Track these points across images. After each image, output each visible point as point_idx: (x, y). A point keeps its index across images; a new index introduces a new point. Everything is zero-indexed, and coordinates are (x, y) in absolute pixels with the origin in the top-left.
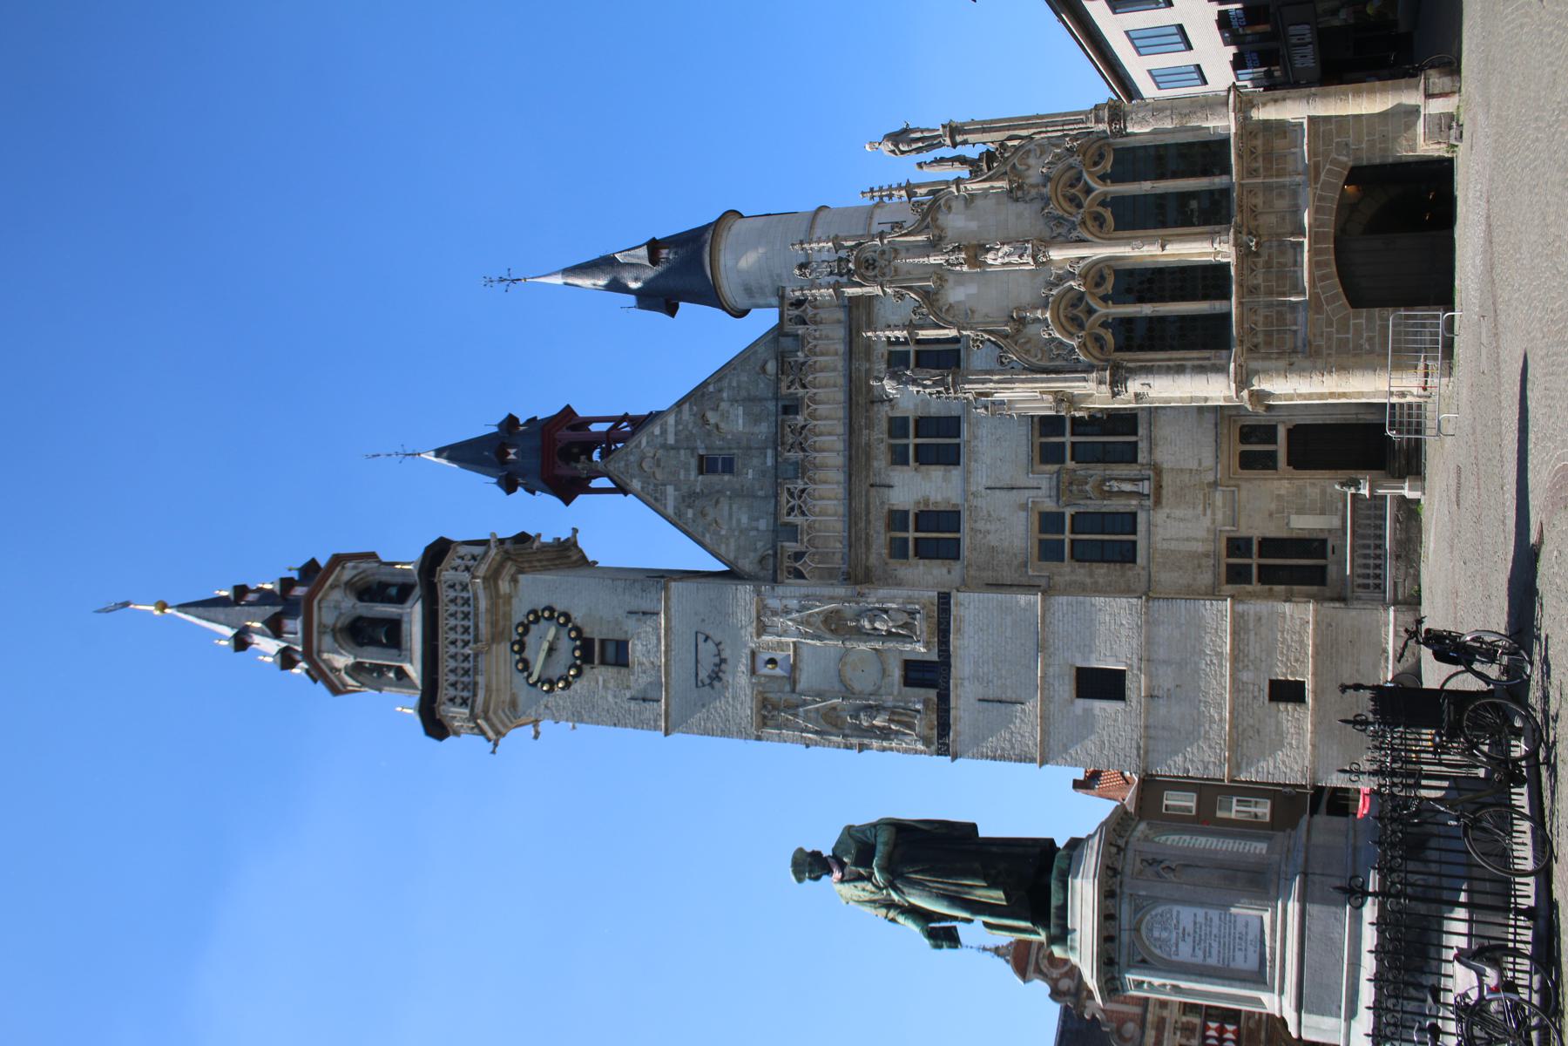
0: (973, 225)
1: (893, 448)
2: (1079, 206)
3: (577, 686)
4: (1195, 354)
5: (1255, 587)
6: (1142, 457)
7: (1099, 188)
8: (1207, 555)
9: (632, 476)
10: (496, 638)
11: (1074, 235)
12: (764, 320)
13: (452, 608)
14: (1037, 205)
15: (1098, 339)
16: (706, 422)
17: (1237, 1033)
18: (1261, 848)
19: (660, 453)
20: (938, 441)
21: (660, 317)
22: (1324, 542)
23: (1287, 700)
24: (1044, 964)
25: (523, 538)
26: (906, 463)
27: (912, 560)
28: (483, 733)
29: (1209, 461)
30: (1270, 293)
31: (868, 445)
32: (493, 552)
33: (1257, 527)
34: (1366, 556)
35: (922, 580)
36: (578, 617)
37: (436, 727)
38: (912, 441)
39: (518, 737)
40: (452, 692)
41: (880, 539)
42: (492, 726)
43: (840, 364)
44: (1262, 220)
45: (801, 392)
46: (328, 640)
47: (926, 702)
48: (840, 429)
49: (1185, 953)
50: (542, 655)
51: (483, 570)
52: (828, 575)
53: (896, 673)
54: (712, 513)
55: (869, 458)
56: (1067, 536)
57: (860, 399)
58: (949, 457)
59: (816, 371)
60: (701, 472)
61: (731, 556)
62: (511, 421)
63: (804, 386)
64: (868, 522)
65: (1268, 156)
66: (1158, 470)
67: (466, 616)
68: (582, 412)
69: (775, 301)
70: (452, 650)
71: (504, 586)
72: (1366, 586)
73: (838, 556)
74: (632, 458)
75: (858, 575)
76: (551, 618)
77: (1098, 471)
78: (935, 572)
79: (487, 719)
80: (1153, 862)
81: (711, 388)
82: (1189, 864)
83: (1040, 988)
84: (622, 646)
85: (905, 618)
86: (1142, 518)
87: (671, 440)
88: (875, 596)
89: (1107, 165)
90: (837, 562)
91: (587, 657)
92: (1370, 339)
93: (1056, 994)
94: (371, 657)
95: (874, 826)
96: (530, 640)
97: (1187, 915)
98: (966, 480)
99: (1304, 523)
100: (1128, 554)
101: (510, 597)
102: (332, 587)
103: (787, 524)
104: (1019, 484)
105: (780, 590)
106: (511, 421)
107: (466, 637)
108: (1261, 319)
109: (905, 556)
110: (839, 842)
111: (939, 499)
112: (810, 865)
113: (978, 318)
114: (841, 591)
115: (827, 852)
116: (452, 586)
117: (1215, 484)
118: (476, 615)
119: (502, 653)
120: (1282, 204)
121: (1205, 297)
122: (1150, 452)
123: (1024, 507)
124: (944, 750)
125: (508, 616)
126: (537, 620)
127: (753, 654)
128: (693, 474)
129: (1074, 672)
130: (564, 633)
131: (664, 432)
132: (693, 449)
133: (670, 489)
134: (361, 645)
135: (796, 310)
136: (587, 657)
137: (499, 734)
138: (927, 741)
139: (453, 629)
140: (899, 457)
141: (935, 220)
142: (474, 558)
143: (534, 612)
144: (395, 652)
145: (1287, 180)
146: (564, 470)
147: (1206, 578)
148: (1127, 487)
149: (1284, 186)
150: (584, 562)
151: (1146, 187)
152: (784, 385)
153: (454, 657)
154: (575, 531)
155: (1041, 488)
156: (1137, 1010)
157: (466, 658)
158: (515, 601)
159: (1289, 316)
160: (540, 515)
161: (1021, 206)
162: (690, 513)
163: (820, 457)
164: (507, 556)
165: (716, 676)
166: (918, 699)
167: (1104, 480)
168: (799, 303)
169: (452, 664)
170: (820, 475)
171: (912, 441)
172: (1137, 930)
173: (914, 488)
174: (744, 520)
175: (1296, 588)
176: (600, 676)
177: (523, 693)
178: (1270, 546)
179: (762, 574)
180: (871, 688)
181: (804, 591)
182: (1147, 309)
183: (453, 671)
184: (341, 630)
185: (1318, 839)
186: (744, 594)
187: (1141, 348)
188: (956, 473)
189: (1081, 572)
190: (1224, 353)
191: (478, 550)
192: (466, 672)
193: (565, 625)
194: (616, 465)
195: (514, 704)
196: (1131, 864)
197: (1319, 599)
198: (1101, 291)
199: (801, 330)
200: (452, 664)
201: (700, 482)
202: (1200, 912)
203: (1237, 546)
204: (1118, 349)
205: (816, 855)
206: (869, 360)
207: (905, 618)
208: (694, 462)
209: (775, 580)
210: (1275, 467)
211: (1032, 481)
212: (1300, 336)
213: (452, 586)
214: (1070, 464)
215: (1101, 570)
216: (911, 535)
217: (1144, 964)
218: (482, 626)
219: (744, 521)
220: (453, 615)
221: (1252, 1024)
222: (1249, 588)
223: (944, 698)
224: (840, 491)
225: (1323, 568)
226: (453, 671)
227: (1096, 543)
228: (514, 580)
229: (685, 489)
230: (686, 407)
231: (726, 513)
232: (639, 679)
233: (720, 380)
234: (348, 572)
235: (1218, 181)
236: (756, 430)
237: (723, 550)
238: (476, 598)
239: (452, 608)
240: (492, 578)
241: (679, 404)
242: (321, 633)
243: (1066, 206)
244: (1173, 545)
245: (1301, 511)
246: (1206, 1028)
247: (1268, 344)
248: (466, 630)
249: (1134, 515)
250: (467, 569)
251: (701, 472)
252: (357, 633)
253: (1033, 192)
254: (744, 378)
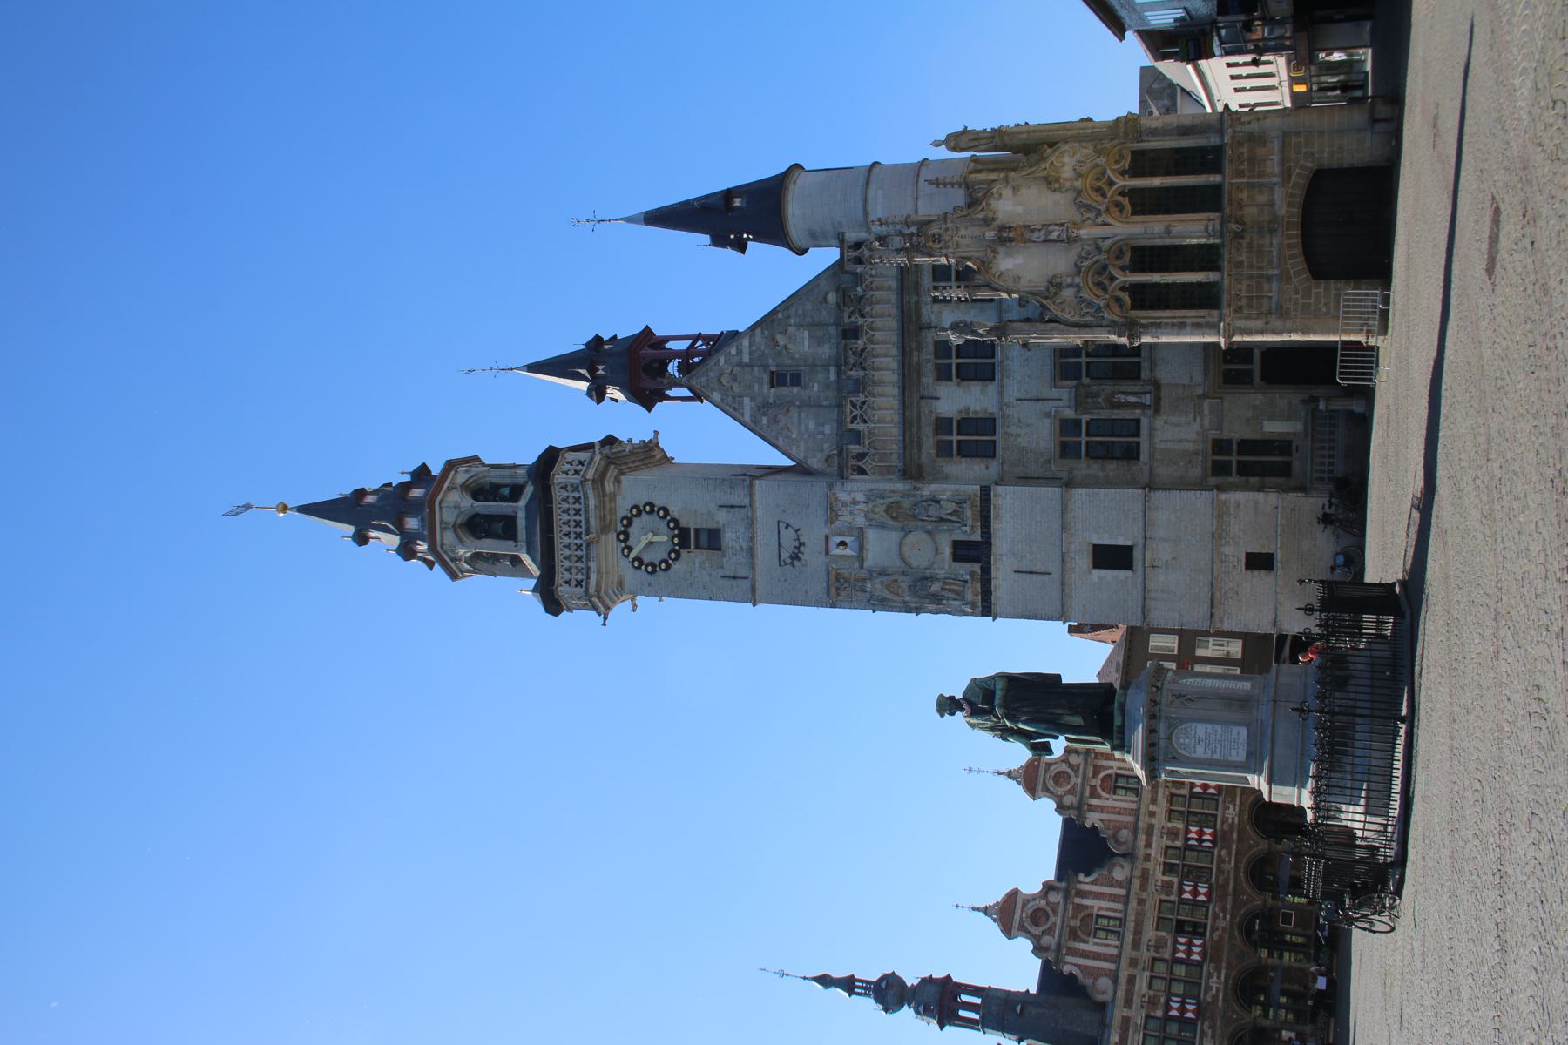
0: (1020, 209)
1: (938, 367)
2: (1104, 195)
3: (676, 566)
4: (1193, 313)
5: (1234, 479)
6: (1145, 374)
7: (1121, 182)
8: (1196, 453)
9: (713, 390)
10: (605, 529)
11: (1100, 220)
12: (824, 257)
13: (565, 506)
14: (1070, 196)
15: (1118, 300)
16: (776, 344)
17: (1214, 835)
18: (1247, 685)
19: (736, 370)
20: (977, 363)
21: (729, 253)
22: (1290, 442)
23: (1259, 568)
24: (1050, 784)
25: (610, 441)
26: (950, 379)
27: (956, 459)
28: (595, 608)
29: (1198, 378)
30: (1251, 267)
31: (918, 364)
32: (597, 458)
33: (1237, 430)
34: (1323, 456)
35: (964, 476)
36: (675, 511)
37: (553, 606)
38: (954, 361)
39: (621, 610)
40: (567, 576)
41: (929, 442)
42: (603, 603)
43: (893, 297)
44: (1247, 210)
45: (861, 321)
46: (449, 537)
47: (972, 574)
48: (895, 351)
49: (1200, 752)
50: (644, 542)
51: (590, 475)
52: (888, 471)
53: (947, 551)
54: (783, 420)
55: (919, 374)
56: (1084, 439)
57: (910, 325)
58: (985, 374)
59: (872, 304)
60: (772, 386)
61: (801, 456)
62: (598, 339)
63: (862, 316)
64: (919, 428)
65: (1252, 160)
66: (1157, 385)
67: (578, 512)
68: (659, 331)
69: (836, 242)
70: (566, 540)
71: (609, 486)
72: (1322, 479)
73: (894, 457)
75: (912, 472)
76: (652, 511)
77: (1108, 387)
78: (976, 468)
79: (599, 598)
80: (1179, 696)
81: (780, 315)
82: (1202, 696)
83: (1047, 805)
85: (953, 507)
86: (1144, 422)
87: (746, 359)
88: (928, 490)
89: (1126, 164)
90: (895, 460)
91: (684, 543)
92: (1326, 304)
93: (1060, 808)
94: (488, 546)
95: (992, 678)
96: (632, 530)
97: (1201, 729)
98: (1001, 393)
99: (1274, 428)
100: (1132, 453)
101: (614, 495)
102: (449, 489)
103: (851, 430)
104: (1044, 396)
105: (849, 486)
106: (598, 339)
107: (578, 530)
108: (1244, 287)
109: (950, 455)
110: (968, 689)
111: (978, 408)
112: (948, 705)
113: (1023, 282)
114: (900, 486)
115: (959, 696)
116: (564, 488)
117: (1204, 396)
118: (587, 512)
119: (610, 542)
120: (1262, 198)
121: (1202, 269)
122: (1152, 370)
123: (1048, 415)
124: (987, 610)
125: (613, 511)
126: (639, 514)
127: (827, 537)
128: (766, 386)
131: (739, 352)
132: (766, 366)
133: (746, 401)
134: (480, 538)
135: (855, 252)
136: (684, 543)
137: (608, 608)
138: (973, 605)
139: (567, 523)
140: (943, 374)
141: (988, 204)
142: (581, 463)
143: (637, 507)
144: (511, 543)
145: (1266, 180)
146: (648, 384)
147: (1196, 472)
148: (1132, 399)
149: (1262, 185)
150: (666, 460)
151: (1157, 182)
152: (846, 314)
153: (568, 546)
154: (657, 433)
155: (1062, 400)
156: (1130, 819)
157: (579, 547)
158: (618, 499)
159: (1266, 286)
161: (1058, 196)
162: (765, 420)
163: (877, 375)
164: (609, 461)
165: (795, 557)
166: (966, 569)
167: (1113, 394)
168: (857, 245)
169: (567, 552)
170: (877, 390)
171: (954, 361)
172: (1169, 738)
173: (954, 399)
174: (812, 425)
175: (1267, 479)
176: (693, 559)
177: (630, 575)
178: (1246, 446)
179: (829, 470)
180: (926, 564)
181: (869, 486)
182: (1156, 278)
183: (568, 558)
184: (461, 526)
185: (1282, 679)
186: (818, 488)
187: (1152, 308)
188: (992, 388)
189: (1095, 468)
190: (1216, 312)
191: (584, 456)
192: (579, 559)
193: (664, 517)
194: (698, 381)
195: (621, 584)
196: (1165, 697)
197: (1283, 489)
198: (1121, 263)
199: (859, 269)
200: (567, 552)
201: (772, 394)
202: (1210, 727)
203: (1220, 446)
204: (1133, 308)
205: (952, 698)
206: (918, 294)
207: (953, 507)
208: (766, 378)
209: (842, 476)
210: (1251, 382)
211: (1055, 393)
212: (1274, 300)
213: (564, 488)
214: (1086, 380)
215: (1111, 466)
216: (955, 438)
217: (1175, 760)
218: (592, 520)
219: (815, 431)
220: (567, 511)
221: (1226, 827)
222: (1230, 479)
223: (986, 570)
224: (896, 403)
225: (1289, 464)
226: (568, 558)
227: (1102, 444)
228: (618, 481)
229: (759, 400)
230: (758, 331)
231: (795, 420)
232: (733, 561)
233: (787, 308)
234: (461, 476)
235: (1214, 179)
236: (820, 350)
237: (794, 451)
238: (586, 498)
239: (565, 506)
240: (599, 480)
241: (753, 328)
242: (442, 529)
243: (1093, 195)
244: (1170, 446)
245: (1271, 418)
246: (1187, 831)
247: (1249, 306)
248: (578, 524)
249: (1138, 421)
250: (577, 472)
251: (772, 386)
252: (476, 526)
253: (1068, 185)
254: (808, 307)
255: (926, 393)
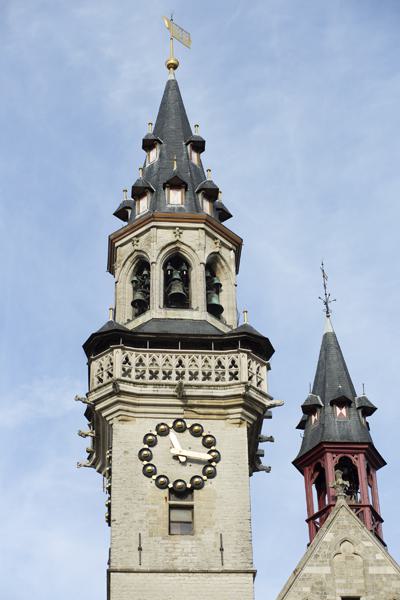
3: (150, 483)
36: (210, 484)
74: (352, 532)
84: (188, 527)
87: (372, 570)
101: (224, 417)
130: (197, 470)
131: (379, 563)
133: (327, 570)
143: (213, 443)
160: (285, 438)
229: (329, 585)
232: (160, 549)
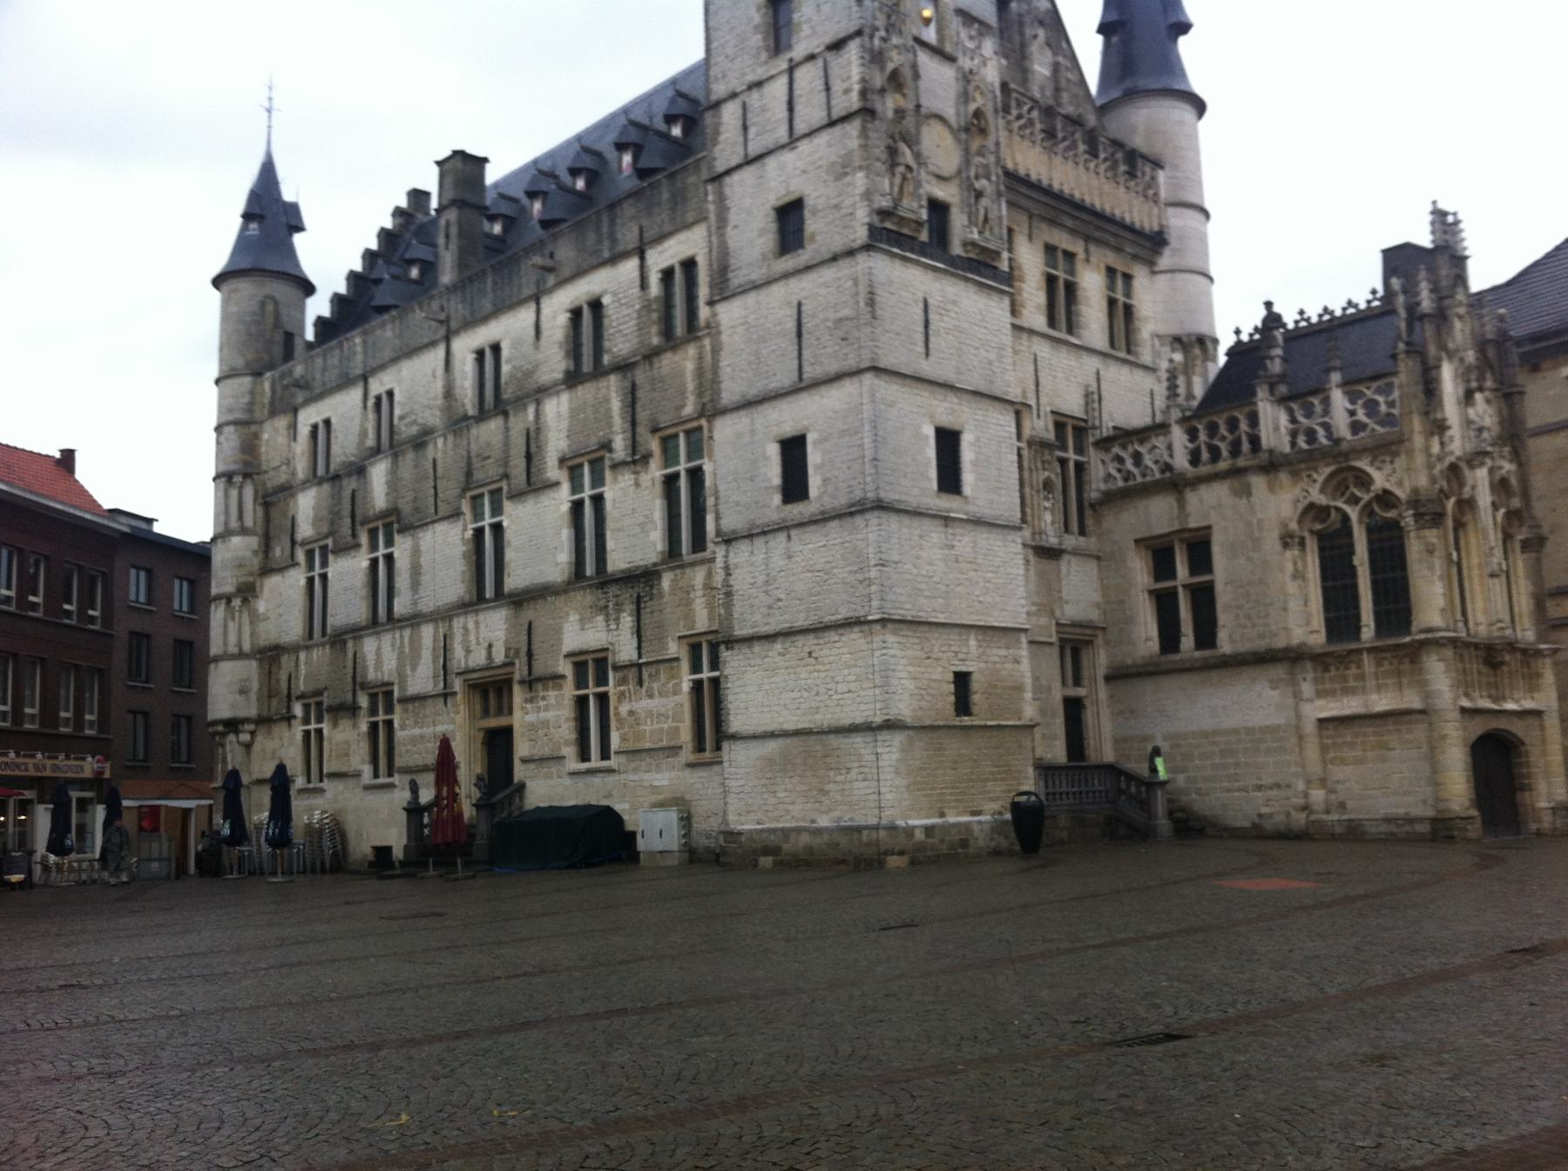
53: (941, 192)
81: (1064, 45)
123: (1024, 393)
129: (956, 427)
255: (1035, 223)
